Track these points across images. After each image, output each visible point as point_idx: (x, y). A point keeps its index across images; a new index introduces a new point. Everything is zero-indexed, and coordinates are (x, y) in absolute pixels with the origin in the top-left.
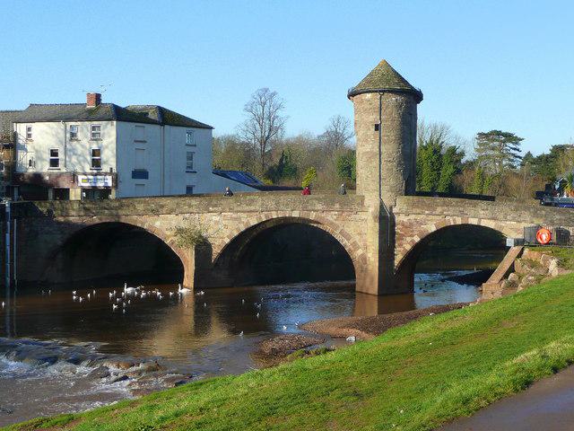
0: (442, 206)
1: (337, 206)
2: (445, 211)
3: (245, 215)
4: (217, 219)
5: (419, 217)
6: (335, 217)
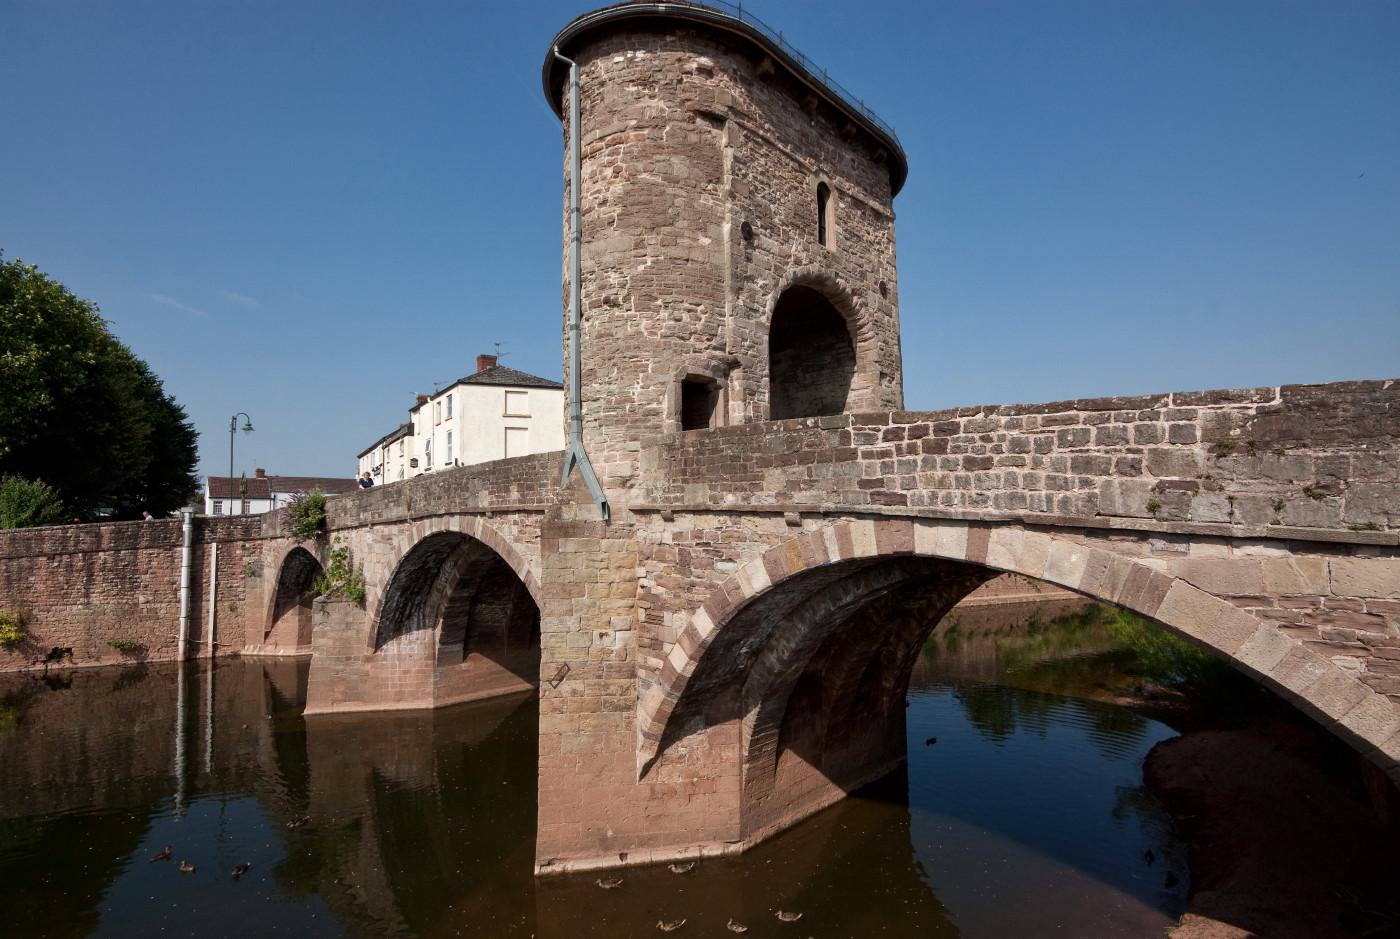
0: (785, 462)
1: (515, 494)
2: (794, 485)
3: (394, 529)
4: (370, 541)
5: (709, 523)
6: (515, 530)
